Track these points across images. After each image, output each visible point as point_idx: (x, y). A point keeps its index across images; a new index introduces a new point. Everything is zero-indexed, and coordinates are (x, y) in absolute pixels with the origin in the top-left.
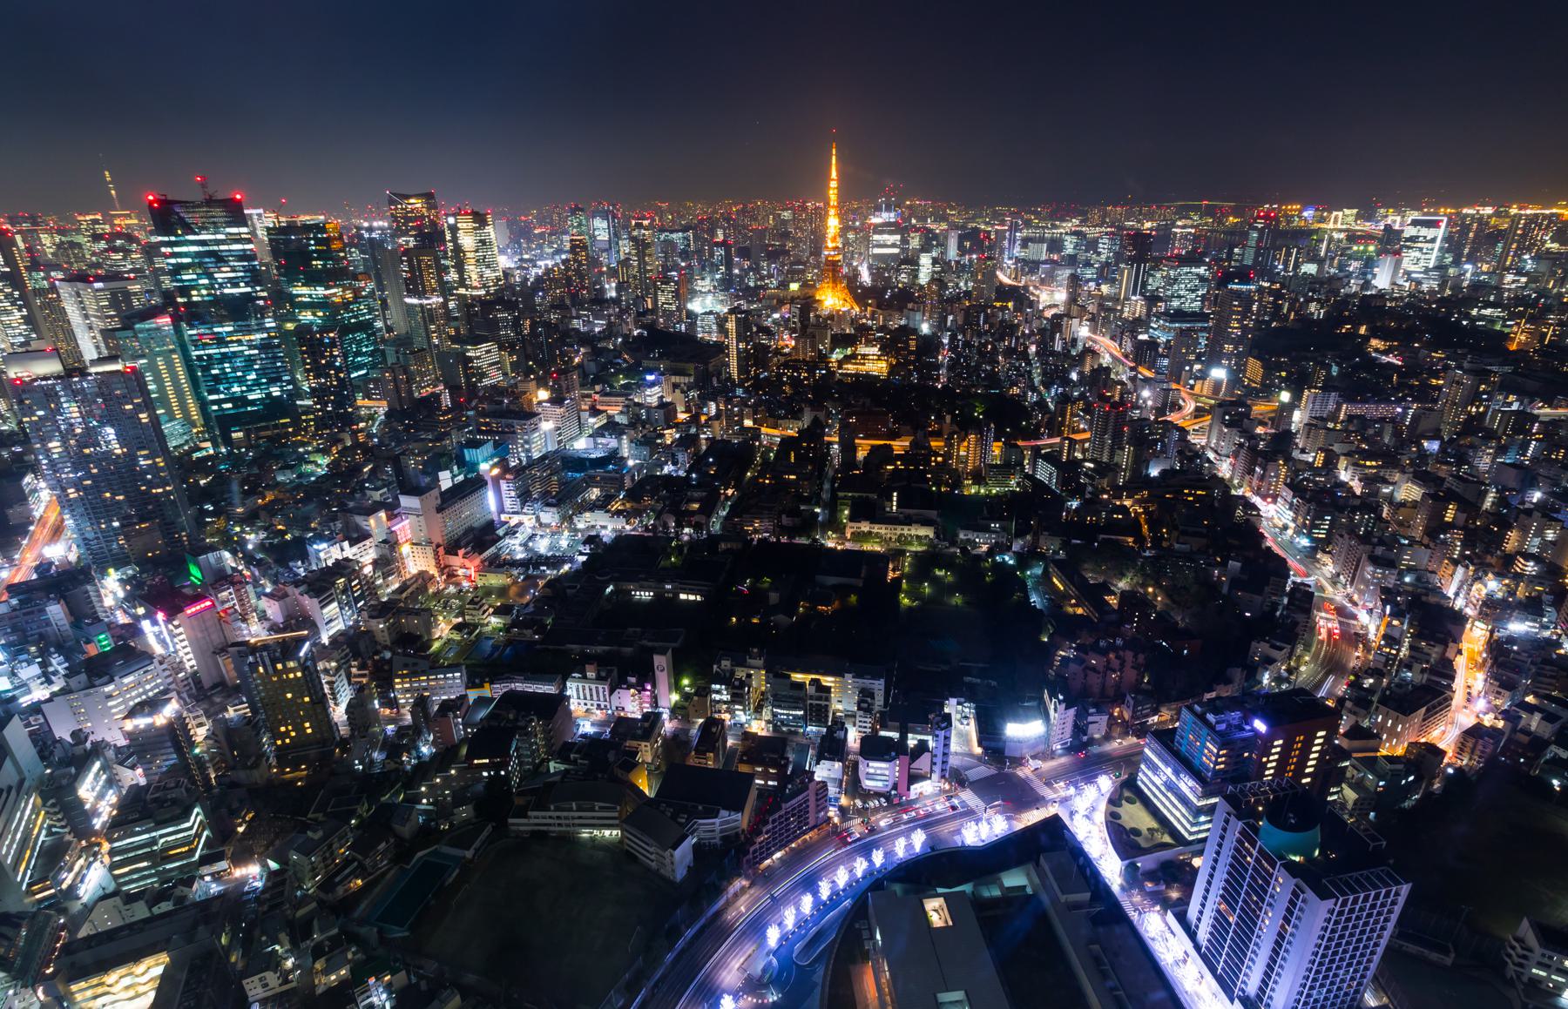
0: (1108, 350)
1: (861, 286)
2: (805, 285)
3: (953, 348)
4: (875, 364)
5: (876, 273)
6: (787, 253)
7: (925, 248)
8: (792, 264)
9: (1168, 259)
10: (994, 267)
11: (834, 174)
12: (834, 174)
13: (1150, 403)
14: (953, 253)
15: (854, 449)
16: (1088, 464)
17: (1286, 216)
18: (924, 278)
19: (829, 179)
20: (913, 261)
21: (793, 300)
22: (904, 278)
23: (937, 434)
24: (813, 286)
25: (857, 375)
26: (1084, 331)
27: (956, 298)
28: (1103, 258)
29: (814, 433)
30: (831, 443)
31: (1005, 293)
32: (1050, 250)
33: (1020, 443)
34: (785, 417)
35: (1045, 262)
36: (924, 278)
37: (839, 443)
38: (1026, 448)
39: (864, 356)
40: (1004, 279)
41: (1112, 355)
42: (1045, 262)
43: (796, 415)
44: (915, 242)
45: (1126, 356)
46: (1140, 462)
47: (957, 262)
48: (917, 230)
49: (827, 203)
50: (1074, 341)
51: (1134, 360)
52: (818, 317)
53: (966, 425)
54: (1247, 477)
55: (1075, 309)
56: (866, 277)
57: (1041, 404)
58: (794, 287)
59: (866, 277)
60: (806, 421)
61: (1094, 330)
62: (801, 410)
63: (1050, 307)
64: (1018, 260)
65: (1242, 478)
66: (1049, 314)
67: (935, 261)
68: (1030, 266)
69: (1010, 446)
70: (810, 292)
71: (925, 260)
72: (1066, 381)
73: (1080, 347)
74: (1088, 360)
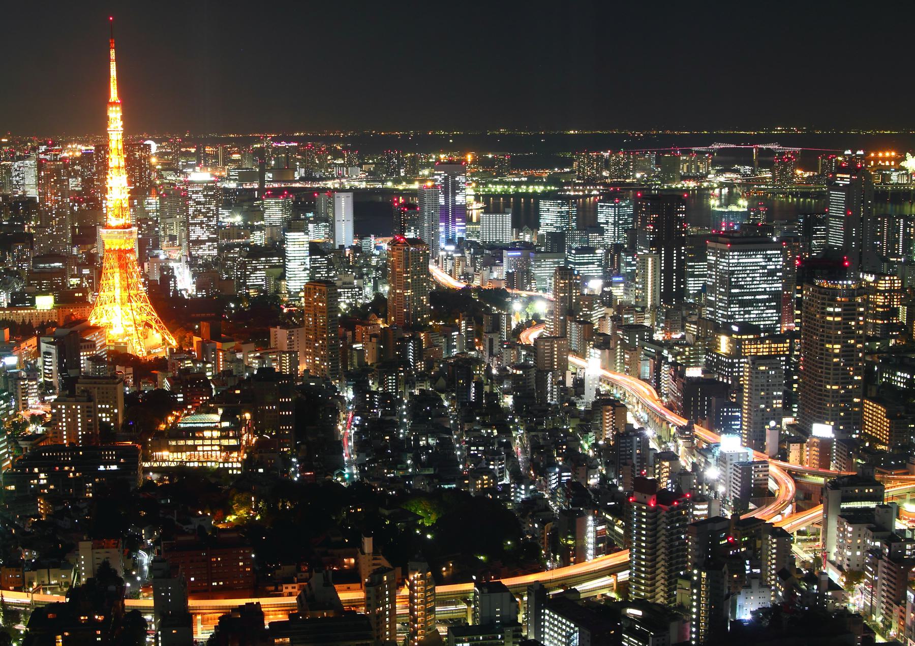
0: (643, 401)
1: (178, 299)
2: (65, 298)
3: (362, 408)
4: (210, 445)
5: (204, 272)
6: (27, 239)
7: (294, 224)
8: (38, 259)
9: (715, 238)
10: (427, 259)
11: (114, 95)
12: (114, 95)
13: (721, 489)
14: (345, 235)
15: (186, 620)
16: (631, 611)
17: (880, 169)
18: (297, 279)
19: (105, 102)
20: (276, 248)
21: (42, 328)
22: (258, 278)
23: (351, 577)
24: (83, 302)
25: (181, 470)
26: (591, 367)
27: (359, 316)
28: (609, 238)
29: (104, 589)
30: (137, 613)
31: (449, 303)
32: (517, 225)
33: (506, 582)
34: (36, 567)
35: (512, 247)
36: (297, 279)
37: (157, 610)
38: (518, 590)
39: (193, 433)
40: (443, 276)
41: (645, 407)
42: (512, 247)
43: (56, 558)
44: (274, 213)
45: (670, 407)
46: (720, 603)
47: (356, 249)
48: (276, 193)
49: (103, 147)
50: (580, 384)
51: (684, 415)
52: (95, 360)
53: (401, 554)
54: (896, 610)
55: (574, 329)
56: (185, 282)
57: (535, 505)
58: (45, 303)
59: (185, 282)
60: (81, 573)
61: (609, 364)
62: (72, 548)
63: (528, 325)
64: (461, 245)
65: (888, 613)
66: (530, 336)
67: (314, 248)
68: (491, 253)
69: (490, 589)
70: (76, 313)
71: (297, 245)
72: (578, 463)
73: (590, 396)
74: (608, 416)
